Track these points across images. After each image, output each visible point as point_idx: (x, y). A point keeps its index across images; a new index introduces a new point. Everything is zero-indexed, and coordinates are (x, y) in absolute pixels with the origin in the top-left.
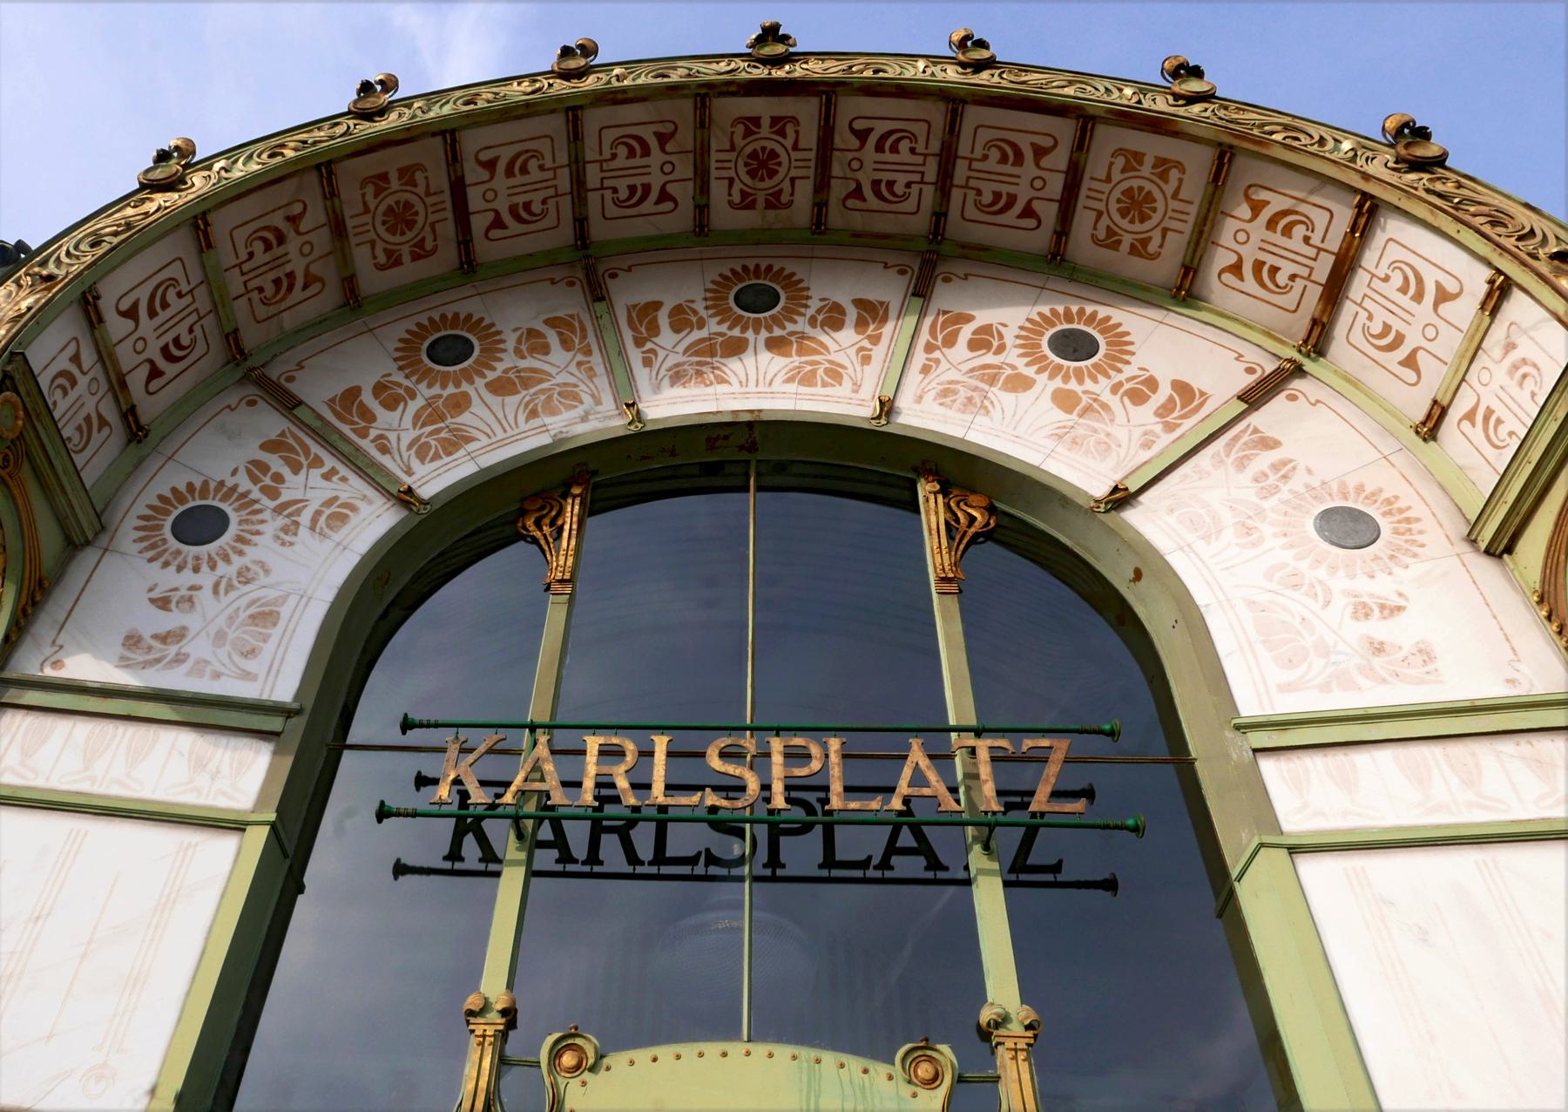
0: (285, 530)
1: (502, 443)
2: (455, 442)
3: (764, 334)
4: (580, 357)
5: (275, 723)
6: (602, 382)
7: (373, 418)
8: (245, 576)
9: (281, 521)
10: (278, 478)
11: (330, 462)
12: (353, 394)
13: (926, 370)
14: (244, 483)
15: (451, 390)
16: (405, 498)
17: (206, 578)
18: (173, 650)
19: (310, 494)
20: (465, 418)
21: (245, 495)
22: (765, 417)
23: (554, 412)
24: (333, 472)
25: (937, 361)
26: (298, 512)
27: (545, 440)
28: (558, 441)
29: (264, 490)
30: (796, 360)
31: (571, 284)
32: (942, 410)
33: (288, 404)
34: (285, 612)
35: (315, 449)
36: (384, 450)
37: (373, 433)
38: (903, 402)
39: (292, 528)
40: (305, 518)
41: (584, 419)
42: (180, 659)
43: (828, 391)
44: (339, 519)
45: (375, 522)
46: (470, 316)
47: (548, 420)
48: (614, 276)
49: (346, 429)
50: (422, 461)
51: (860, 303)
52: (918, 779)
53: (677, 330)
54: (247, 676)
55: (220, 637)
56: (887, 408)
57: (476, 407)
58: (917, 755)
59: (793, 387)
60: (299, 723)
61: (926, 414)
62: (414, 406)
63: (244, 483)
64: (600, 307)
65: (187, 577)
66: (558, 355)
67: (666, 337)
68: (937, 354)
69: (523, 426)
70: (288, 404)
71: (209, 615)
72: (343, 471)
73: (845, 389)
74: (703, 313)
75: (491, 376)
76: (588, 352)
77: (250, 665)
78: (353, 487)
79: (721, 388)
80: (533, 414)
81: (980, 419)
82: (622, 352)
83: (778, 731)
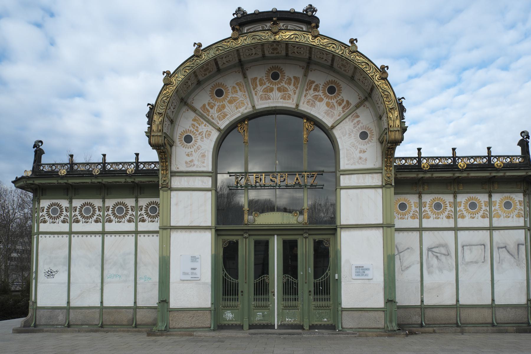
0: (202, 138)
1: (232, 116)
2: (225, 116)
3: (277, 86)
4: (244, 93)
5: (211, 174)
6: (248, 99)
7: (209, 112)
8: (198, 148)
9: (200, 137)
10: (197, 127)
11: (205, 122)
12: (204, 105)
13: (305, 96)
14: (191, 128)
15: (221, 103)
16: (219, 130)
17: (192, 150)
18: (192, 164)
19: (204, 130)
20: (225, 110)
21: (193, 132)
22: (277, 108)
23: (241, 108)
24: (206, 125)
25: (307, 94)
26: (202, 134)
27: (239, 114)
28: (242, 115)
29: (196, 130)
30: (283, 93)
31: (239, 73)
32: (307, 106)
33: (194, 110)
34: (206, 154)
35: (202, 120)
36: (213, 119)
37: (210, 115)
38: (301, 104)
39: (202, 138)
40: (204, 135)
41: (246, 109)
42: (194, 165)
43: (288, 101)
44: (209, 135)
45: (215, 135)
46: (221, 84)
47: (240, 109)
48: (247, 70)
49: (205, 114)
50: (220, 120)
51: (294, 77)
52: (297, 179)
53: (261, 86)
54: (204, 167)
55: (198, 160)
56: (297, 105)
57: (227, 108)
58: (297, 176)
59: (282, 100)
60: (214, 174)
61: (305, 108)
62: (216, 107)
63: (191, 128)
64: (246, 79)
65: (190, 150)
66: (240, 93)
67: (259, 88)
68: (307, 92)
69: (236, 111)
70: (194, 110)
71: (195, 156)
72: (207, 124)
73: (291, 101)
74: (265, 80)
75: (228, 99)
76: (245, 92)
77: (204, 165)
78: (210, 128)
79: (269, 101)
80: (237, 108)
81: (313, 108)
82: (251, 92)
83: (279, 172)
